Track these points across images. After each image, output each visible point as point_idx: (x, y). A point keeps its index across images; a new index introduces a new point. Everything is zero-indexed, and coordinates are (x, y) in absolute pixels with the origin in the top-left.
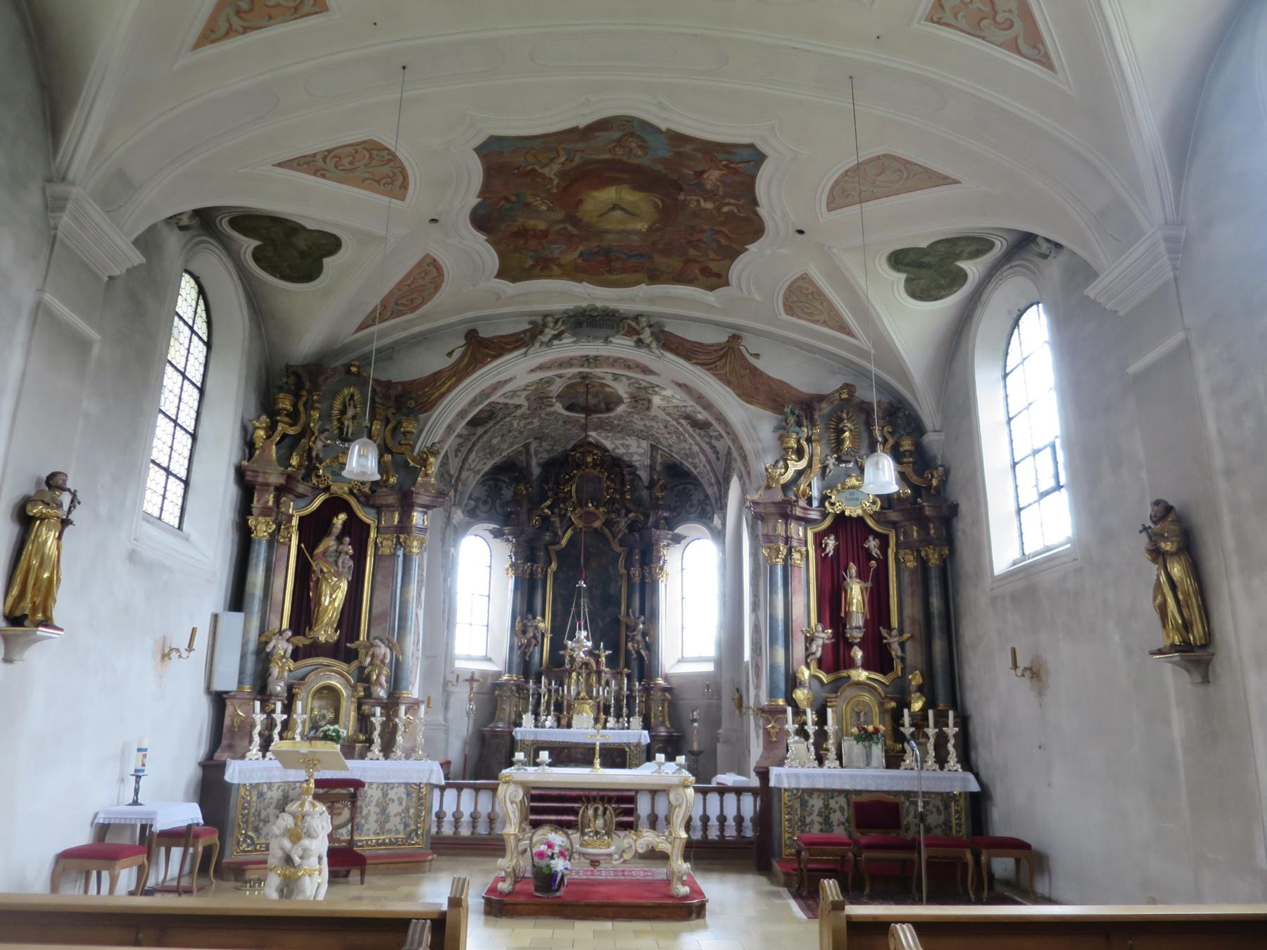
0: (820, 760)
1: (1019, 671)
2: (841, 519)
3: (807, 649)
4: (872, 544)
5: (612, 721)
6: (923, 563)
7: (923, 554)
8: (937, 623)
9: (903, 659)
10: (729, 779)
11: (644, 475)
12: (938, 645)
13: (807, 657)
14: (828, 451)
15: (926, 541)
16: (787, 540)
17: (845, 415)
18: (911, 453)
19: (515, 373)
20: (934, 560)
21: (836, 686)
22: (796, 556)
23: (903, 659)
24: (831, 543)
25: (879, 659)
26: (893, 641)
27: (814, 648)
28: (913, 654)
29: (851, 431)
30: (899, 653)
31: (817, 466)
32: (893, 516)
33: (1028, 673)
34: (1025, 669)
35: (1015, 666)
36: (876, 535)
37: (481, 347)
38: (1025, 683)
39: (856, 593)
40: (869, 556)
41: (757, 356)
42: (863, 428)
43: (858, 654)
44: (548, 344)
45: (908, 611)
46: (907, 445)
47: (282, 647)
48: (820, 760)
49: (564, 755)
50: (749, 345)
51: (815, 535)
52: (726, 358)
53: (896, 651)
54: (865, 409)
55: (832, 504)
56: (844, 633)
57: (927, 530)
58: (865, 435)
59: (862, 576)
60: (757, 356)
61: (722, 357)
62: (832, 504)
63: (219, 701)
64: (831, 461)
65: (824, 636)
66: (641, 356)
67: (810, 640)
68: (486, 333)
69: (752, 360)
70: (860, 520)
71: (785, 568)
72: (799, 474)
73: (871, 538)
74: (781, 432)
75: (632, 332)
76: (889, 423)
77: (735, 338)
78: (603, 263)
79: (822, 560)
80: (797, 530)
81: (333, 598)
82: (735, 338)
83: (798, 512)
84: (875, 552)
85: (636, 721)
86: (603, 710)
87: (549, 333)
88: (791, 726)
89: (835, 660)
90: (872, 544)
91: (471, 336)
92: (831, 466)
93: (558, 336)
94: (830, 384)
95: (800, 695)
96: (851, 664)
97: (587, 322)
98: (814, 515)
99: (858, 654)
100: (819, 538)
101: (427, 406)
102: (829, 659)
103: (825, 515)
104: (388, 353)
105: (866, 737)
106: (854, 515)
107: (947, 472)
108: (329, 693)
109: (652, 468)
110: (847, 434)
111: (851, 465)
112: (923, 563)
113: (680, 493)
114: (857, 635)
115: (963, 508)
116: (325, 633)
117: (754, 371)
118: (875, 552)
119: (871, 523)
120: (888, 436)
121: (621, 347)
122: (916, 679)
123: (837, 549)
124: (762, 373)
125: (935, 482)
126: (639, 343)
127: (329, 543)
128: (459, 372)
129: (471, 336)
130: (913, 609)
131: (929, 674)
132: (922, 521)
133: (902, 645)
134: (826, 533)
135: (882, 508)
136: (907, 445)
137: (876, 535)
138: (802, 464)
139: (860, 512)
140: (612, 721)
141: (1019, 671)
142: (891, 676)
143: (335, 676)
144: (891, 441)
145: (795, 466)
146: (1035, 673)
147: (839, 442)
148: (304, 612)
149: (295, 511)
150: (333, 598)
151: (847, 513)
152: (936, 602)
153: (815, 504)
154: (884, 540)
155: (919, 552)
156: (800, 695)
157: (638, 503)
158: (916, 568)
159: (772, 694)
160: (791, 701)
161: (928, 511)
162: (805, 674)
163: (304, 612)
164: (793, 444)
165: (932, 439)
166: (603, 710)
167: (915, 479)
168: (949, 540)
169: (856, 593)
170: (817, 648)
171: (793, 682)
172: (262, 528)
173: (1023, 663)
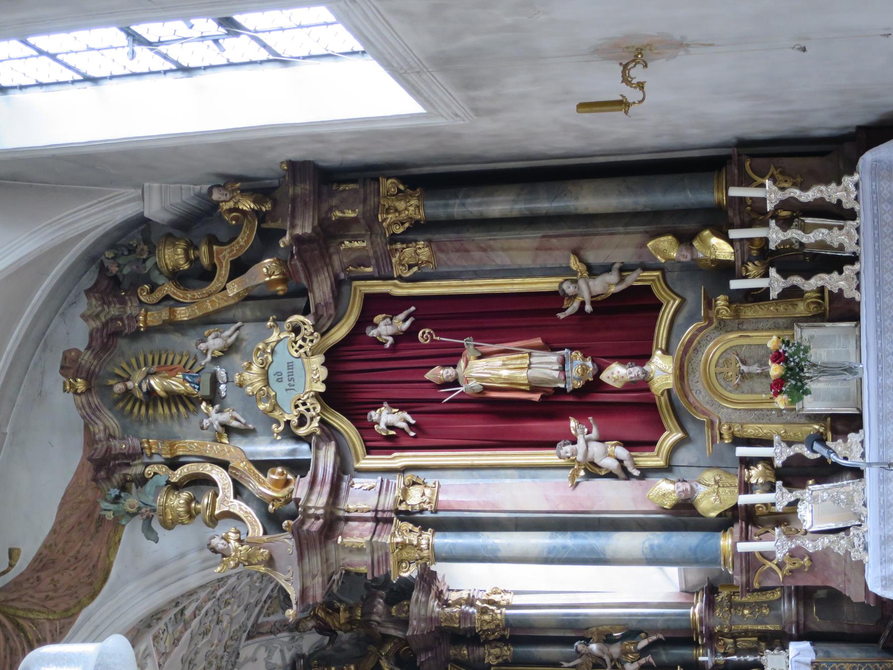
1: (632, 95)
2: (336, 396)
3: (611, 475)
4: (385, 329)
7: (399, 230)
8: (544, 205)
9: (625, 269)
12: (589, 200)
13: (628, 476)
14: (195, 420)
15: (371, 223)
16: (380, 520)
17: (119, 388)
18: (191, 246)
20: (411, 208)
22: (415, 498)
23: (625, 269)
24: (386, 418)
25: (624, 323)
26: (589, 289)
27: (610, 463)
29: (149, 374)
30: (613, 277)
32: (321, 290)
33: (637, 73)
34: (626, 80)
35: (622, 104)
36: (365, 320)
38: (656, 76)
39: (492, 369)
41: (13, 554)
42: (143, 346)
45: (524, 260)
46: (174, 256)
51: (369, 450)
53: (607, 284)
54: (107, 338)
55: (302, 421)
56: (575, 392)
57: (344, 223)
58: (159, 340)
59: (452, 357)
60: (13, 554)
61: (18, 627)
62: (302, 421)
64: (215, 417)
65: (587, 441)
67: (593, 471)
69: (23, 564)
70: (334, 358)
71: (441, 526)
73: (372, 333)
74: (155, 524)
76: (133, 290)
79: (422, 437)
80: (361, 495)
83: (319, 500)
84: (401, 323)
88: (773, 544)
90: (385, 329)
92: (225, 417)
94: (62, 404)
96: (642, 386)
98: (327, 458)
99: (617, 373)
100: (380, 444)
103: (328, 432)
106: (323, 373)
107: (228, 181)
110: (155, 383)
111: (222, 373)
114: (579, 367)
115: (295, 154)
117: (43, 562)
118: (401, 323)
119: (339, 333)
120: (158, 295)
122: (666, 247)
123: (397, 404)
124: (45, 546)
125: (247, 205)
130: (519, 248)
131: (655, 221)
132: (329, 233)
133: (593, 271)
134: (365, 428)
135: (306, 312)
136: (174, 256)
137: (365, 320)
139: (318, 360)
141: (632, 95)
142: (660, 292)
144: (169, 288)
145: (226, 501)
146: (634, 56)
147: (173, 398)
151: (322, 388)
152: (500, 205)
153: (304, 451)
154: (376, 305)
155: (394, 239)
158: (429, 242)
161: (305, 227)
162: (665, 490)
164: (178, 501)
165: (158, 207)
167: (245, 240)
168: (362, 176)
169: (492, 369)
170: (609, 454)
173: (609, 86)
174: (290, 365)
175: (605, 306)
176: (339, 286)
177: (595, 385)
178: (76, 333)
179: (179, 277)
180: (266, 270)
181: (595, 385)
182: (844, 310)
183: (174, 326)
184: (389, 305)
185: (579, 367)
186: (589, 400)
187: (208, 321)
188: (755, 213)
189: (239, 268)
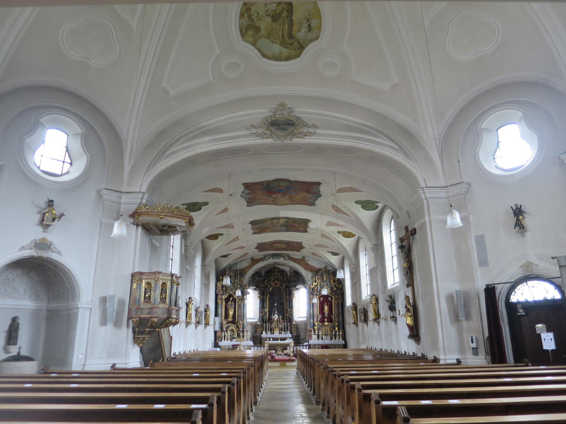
0: (318, 339)
4: (329, 299)
5: (283, 332)
6: (338, 302)
10: (305, 344)
11: (289, 273)
12: (340, 318)
15: (339, 298)
19: (261, 265)
20: (340, 302)
21: (323, 325)
25: (330, 320)
28: (336, 319)
37: (254, 261)
43: (326, 320)
44: (267, 260)
47: (224, 322)
48: (318, 339)
49: (274, 339)
50: (306, 259)
53: (333, 319)
59: (327, 305)
63: (216, 332)
65: (320, 316)
66: (286, 261)
67: (317, 317)
68: (255, 258)
72: (315, 286)
75: (284, 257)
77: (304, 257)
78: (278, 249)
81: (231, 313)
82: (304, 257)
86: (281, 330)
87: (267, 258)
88: (313, 333)
89: (322, 321)
90: (329, 299)
91: (252, 259)
93: (269, 258)
94: (323, 266)
95: (315, 328)
96: (325, 322)
97: (274, 256)
98: (318, 294)
99: (326, 320)
101: (245, 274)
104: (236, 264)
105: (326, 335)
108: (232, 330)
109: (291, 272)
112: (338, 302)
113: (296, 279)
114: (326, 316)
116: (230, 319)
117: (307, 264)
121: (281, 260)
126: (285, 259)
127: (230, 303)
128: (250, 267)
129: (252, 259)
130: (336, 311)
131: (339, 323)
132: (338, 295)
140: (283, 332)
143: (233, 327)
145: (315, 284)
148: (227, 316)
149: (224, 297)
150: (231, 313)
152: (340, 310)
154: (332, 299)
156: (315, 328)
157: (288, 280)
163: (227, 316)
166: (281, 330)
167: (337, 286)
170: (319, 319)
171: (314, 325)
172: (219, 302)
175: (332, 318)
177: (325, 318)
180: (335, 289)
181: (325, 318)
182: (331, 339)
185: (326, 316)
186: (323, 317)
187: (330, 282)
188: (339, 332)
189: (335, 285)
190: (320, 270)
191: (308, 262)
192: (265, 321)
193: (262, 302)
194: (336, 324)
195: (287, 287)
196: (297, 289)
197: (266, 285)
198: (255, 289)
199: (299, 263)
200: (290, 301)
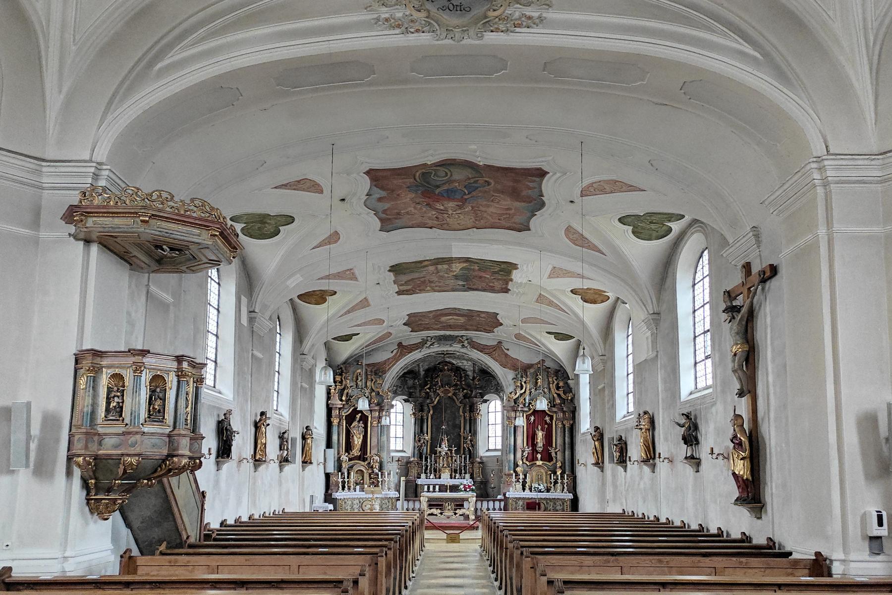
0: (524, 490)
4: (547, 418)
6: (564, 425)
12: (567, 453)
24: (532, 418)
25: (547, 457)
31: (528, 392)
32: (554, 409)
36: (549, 415)
39: (540, 435)
40: (546, 423)
43: (539, 456)
46: (561, 384)
48: (524, 490)
50: (505, 345)
52: (495, 350)
53: (553, 455)
59: (542, 430)
65: (528, 450)
67: (523, 451)
72: (521, 394)
79: (528, 424)
84: (548, 421)
85: (468, 476)
88: (514, 479)
89: (532, 458)
90: (547, 418)
94: (535, 360)
95: (518, 469)
96: (537, 459)
98: (526, 409)
99: (539, 456)
102: (530, 457)
109: (474, 371)
113: (487, 382)
114: (540, 450)
117: (506, 355)
118: (548, 421)
130: (560, 441)
131: (563, 463)
132: (564, 412)
133: (556, 453)
134: (530, 415)
137: (549, 415)
138: (523, 391)
145: (519, 392)
147: (537, 383)
156: (518, 469)
157: (469, 386)
159: (509, 470)
160: (515, 471)
162: (520, 463)
167: (563, 396)
169: (540, 435)
170: (526, 454)
171: (516, 465)
174: (542, 404)
175: (550, 454)
176: (556, 412)
178: (547, 364)
179: (558, 384)
180: (558, 401)
181: (537, 453)
183: (549, 384)
184: (551, 419)
186: (534, 450)
188: (562, 477)
189: (559, 395)
190: (530, 366)
191: (508, 353)
192: (424, 458)
193: (420, 423)
194: (559, 464)
195: (465, 396)
196: (486, 401)
197: (427, 393)
198: (406, 401)
199: (489, 354)
200: (472, 422)
